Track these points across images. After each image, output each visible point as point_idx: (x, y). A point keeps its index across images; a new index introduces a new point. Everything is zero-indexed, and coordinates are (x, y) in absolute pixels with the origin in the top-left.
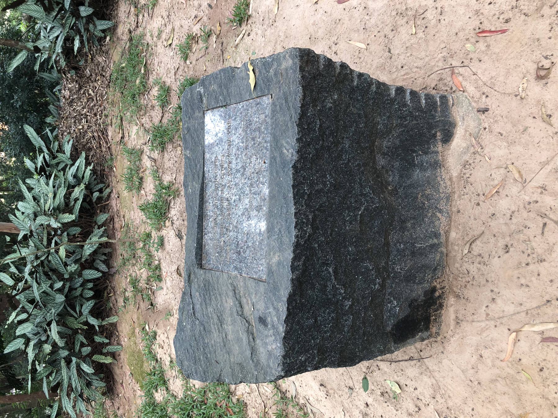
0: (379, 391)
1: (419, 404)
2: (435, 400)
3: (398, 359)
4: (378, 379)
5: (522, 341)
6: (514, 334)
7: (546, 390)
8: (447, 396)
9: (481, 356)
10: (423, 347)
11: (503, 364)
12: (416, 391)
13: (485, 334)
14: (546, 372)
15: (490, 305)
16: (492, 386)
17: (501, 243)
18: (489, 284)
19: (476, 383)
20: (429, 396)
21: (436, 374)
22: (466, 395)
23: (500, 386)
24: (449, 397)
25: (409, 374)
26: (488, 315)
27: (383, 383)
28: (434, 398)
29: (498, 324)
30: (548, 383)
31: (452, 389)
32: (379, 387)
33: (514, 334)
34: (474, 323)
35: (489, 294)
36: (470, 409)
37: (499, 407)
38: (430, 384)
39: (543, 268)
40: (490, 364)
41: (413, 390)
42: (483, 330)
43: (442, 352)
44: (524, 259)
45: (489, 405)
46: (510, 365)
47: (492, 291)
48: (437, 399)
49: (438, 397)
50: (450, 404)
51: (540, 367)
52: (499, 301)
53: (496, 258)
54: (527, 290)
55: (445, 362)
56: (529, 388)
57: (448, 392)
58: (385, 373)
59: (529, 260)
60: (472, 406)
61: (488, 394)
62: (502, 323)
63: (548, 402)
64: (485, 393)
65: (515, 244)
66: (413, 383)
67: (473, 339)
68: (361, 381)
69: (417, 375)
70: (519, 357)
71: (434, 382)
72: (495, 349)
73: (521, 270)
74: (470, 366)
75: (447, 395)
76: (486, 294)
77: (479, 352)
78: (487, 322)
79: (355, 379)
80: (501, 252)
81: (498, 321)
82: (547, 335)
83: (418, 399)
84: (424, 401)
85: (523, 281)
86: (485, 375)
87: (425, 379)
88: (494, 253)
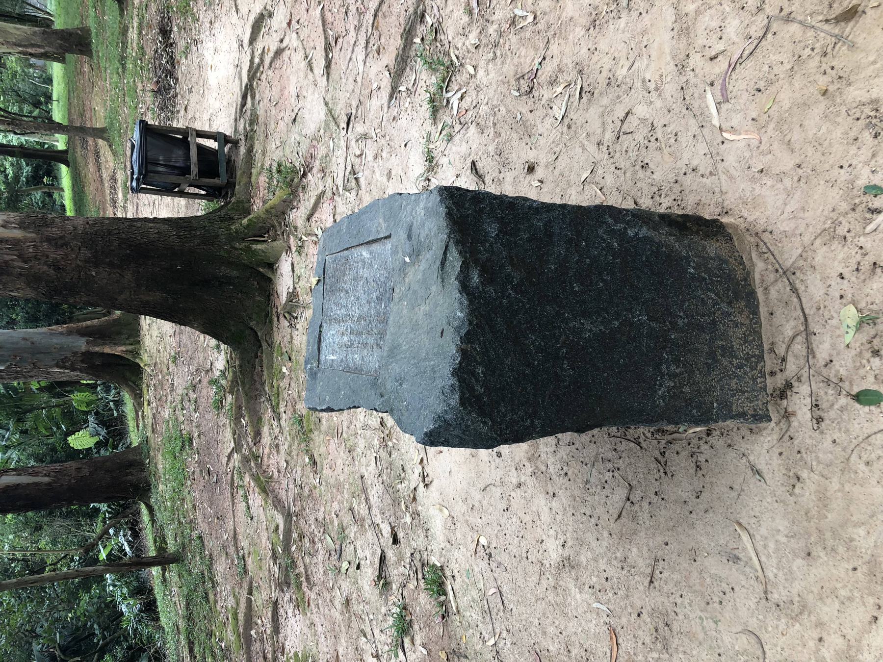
0: (872, 360)
1: (868, 267)
2: (848, 235)
3: (802, 319)
4: (850, 365)
5: (733, 124)
6: (724, 134)
7: (782, 76)
8: (834, 215)
9: (762, 171)
10: (770, 267)
11: (765, 139)
12: (846, 275)
13: (734, 173)
14: (761, 85)
15: (700, 173)
16: (797, 147)
17: (641, 174)
18: (679, 179)
19: (800, 171)
20: (846, 248)
21: (807, 239)
22: (822, 182)
23: (796, 136)
24: (834, 210)
25: (822, 292)
26: (711, 174)
27: (853, 352)
28: (845, 238)
29: (718, 158)
30: (773, 77)
31: (821, 208)
32: (864, 361)
33: (724, 134)
34: (724, 191)
35: (689, 177)
36: (842, 171)
37: (824, 129)
38: (825, 248)
39: (658, 124)
40: (770, 156)
41: (845, 282)
42: (731, 178)
43: (771, 232)
44: (653, 145)
45: (826, 144)
46: (764, 130)
47: (685, 174)
48: (845, 233)
49: (842, 231)
50: (844, 206)
51: (757, 93)
52: (694, 163)
53: (654, 176)
54: (679, 134)
55: (785, 226)
56: (786, 98)
57: (826, 213)
58: (833, 346)
59: (653, 139)
60: (837, 170)
61: (810, 151)
62: (718, 154)
63: (795, 67)
64: (810, 155)
65: (640, 159)
66: (833, 283)
67: (743, 187)
68: (867, 409)
69: (818, 277)
70: (751, 122)
71: (818, 242)
72: (747, 154)
73: (663, 146)
74: (779, 185)
75: (832, 215)
76: (688, 181)
77: (757, 175)
78: (720, 172)
79: (868, 429)
80: (649, 173)
81: (716, 158)
82: (720, 98)
83: (857, 270)
84: (858, 257)
85: (672, 140)
86: (787, 162)
87: (819, 259)
88: (650, 180)
